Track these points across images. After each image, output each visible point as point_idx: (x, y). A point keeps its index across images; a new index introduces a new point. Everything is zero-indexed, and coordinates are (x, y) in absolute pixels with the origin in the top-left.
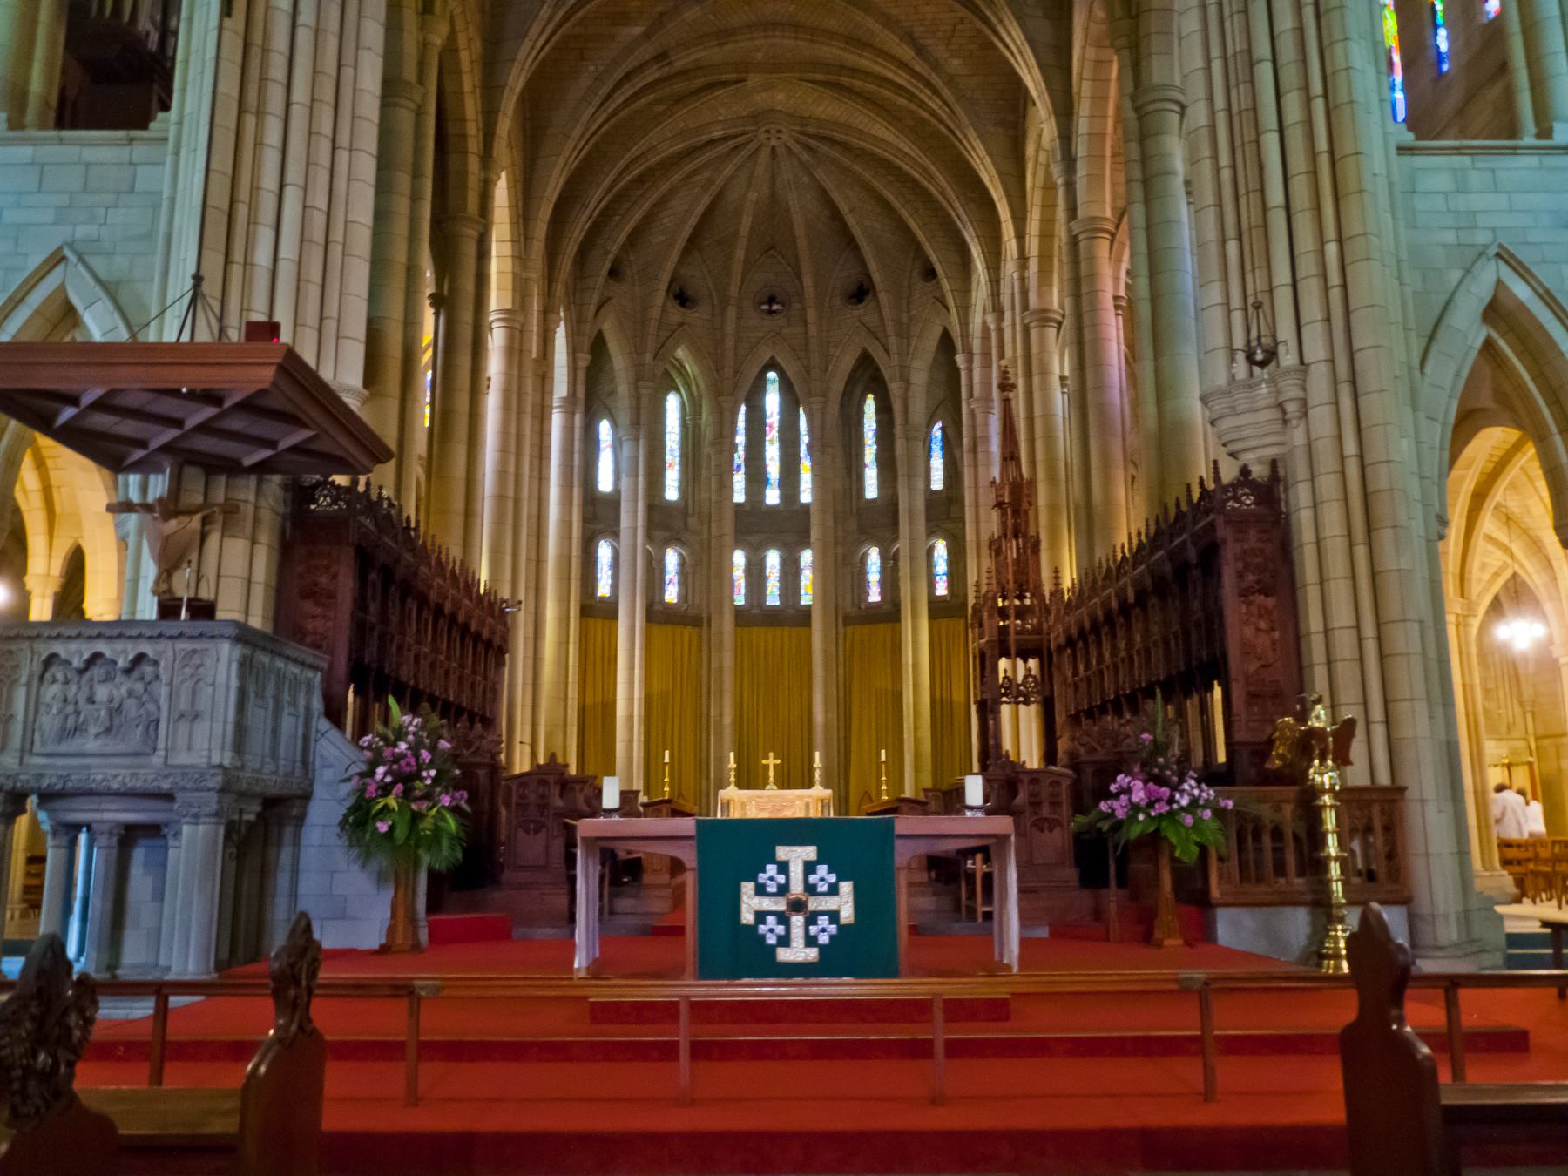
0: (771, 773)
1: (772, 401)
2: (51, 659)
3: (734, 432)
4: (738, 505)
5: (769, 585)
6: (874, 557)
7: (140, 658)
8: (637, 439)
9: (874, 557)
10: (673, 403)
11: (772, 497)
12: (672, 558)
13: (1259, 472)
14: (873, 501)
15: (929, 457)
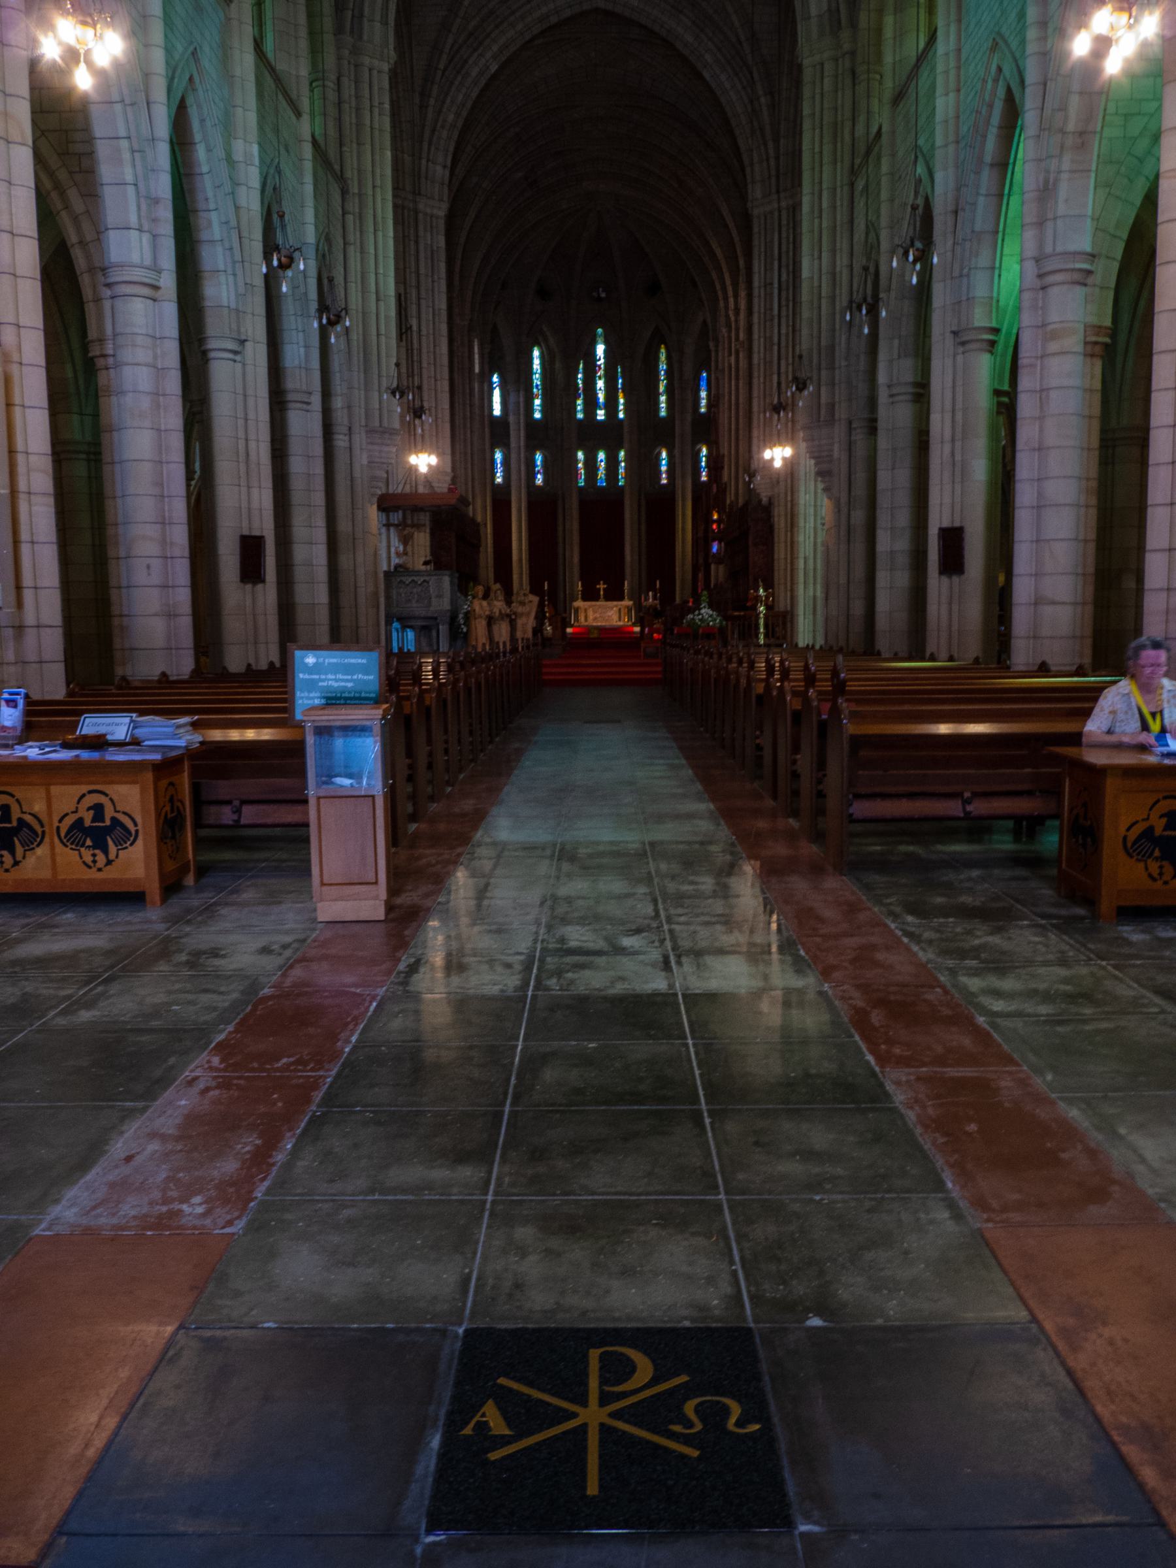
0: (602, 593)
1: (600, 349)
2: (401, 582)
3: (578, 373)
4: (580, 421)
5: (600, 473)
6: (664, 455)
7: (424, 581)
8: (519, 391)
9: (664, 455)
10: (536, 353)
11: (601, 415)
12: (539, 458)
13: (765, 500)
14: (663, 419)
15: (698, 391)
